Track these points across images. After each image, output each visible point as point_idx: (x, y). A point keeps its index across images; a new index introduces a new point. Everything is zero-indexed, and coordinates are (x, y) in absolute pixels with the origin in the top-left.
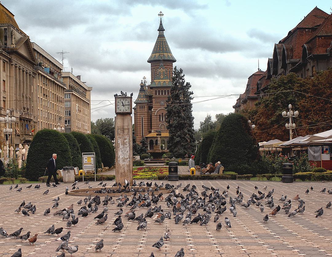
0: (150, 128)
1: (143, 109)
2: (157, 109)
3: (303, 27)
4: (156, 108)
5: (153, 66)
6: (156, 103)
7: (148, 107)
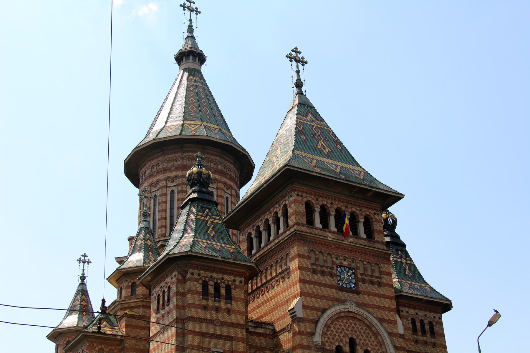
1: (223, 304)
2: (324, 311)
4: (319, 303)
6: (314, 272)
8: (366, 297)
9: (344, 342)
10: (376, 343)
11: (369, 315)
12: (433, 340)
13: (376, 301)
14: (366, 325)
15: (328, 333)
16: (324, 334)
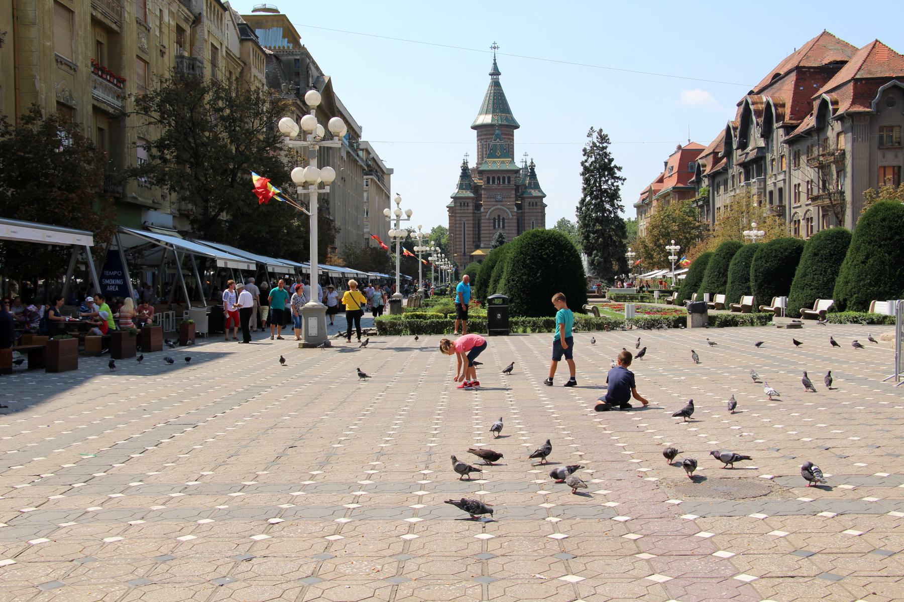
0: (477, 240)
3: (806, 65)
4: (488, 207)
5: (481, 135)
6: (488, 198)
7: (474, 205)
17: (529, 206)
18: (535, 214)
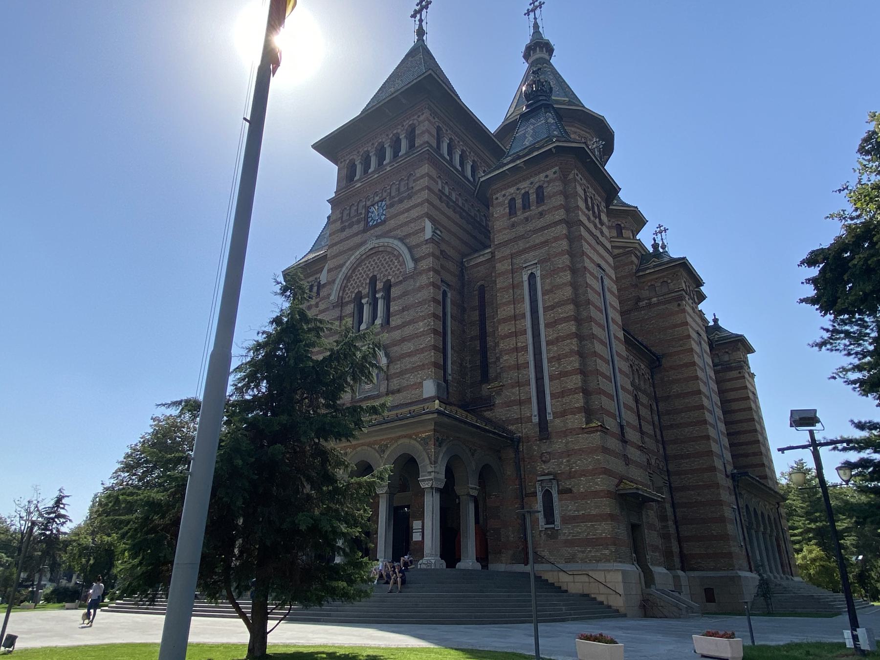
6: (343, 230)
8: (392, 222)
9: (364, 285)
10: (398, 267)
11: (391, 240)
12: (540, 209)
13: (403, 218)
14: (389, 253)
15: (349, 284)
16: (343, 288)
17: (512, 211)
18: (538, 239)
